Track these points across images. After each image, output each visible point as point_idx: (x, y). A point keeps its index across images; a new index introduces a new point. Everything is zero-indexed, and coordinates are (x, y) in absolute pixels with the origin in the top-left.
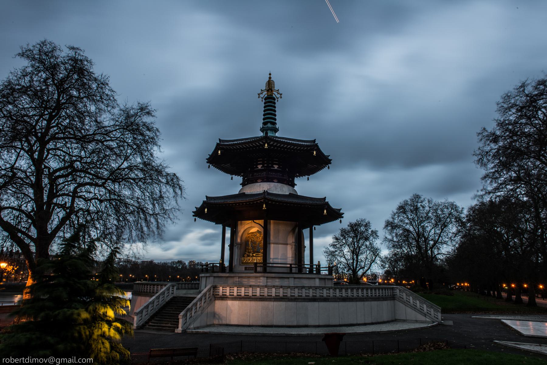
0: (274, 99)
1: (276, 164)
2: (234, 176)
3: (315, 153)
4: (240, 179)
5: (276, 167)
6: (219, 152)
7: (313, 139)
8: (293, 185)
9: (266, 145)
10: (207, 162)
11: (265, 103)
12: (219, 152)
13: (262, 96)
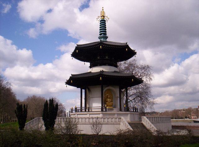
2: (85, 62)
3: (127, 49)
4: (88, 64)
8: (116, 66)
10: (71, 56)
13: (98, 19)
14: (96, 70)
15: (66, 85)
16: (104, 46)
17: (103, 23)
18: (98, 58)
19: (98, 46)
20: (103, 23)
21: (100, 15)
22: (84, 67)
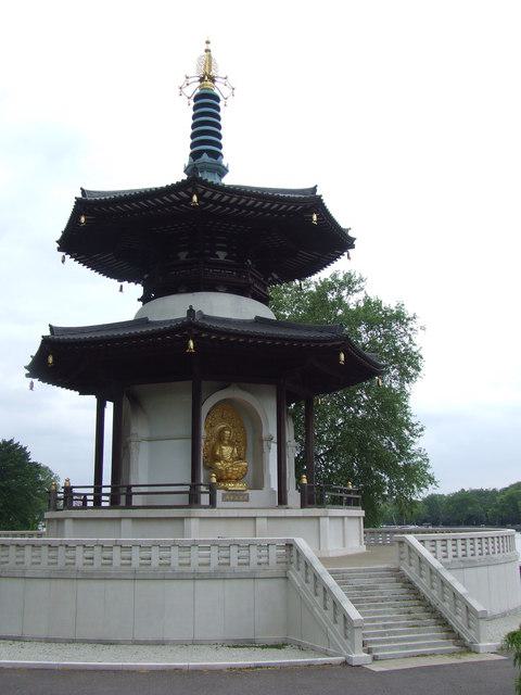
0: (218, 99)
1: (222, 249)
2: (125, 284)
3: (315, 217)
4: (137, 290)
5: (222, 255)
6: (83, 219)
7: (313, 186)
9: (195, 198)
10: (59, 250)
11: (195, 108)
12: (83, 219)
14: (173, 308)
15: (30, 380)
16: (208, 194)
17: (206, 111)
18: (183, 256)
19: (182, 193)
20: (206, 111)
21: (194, 72)
22: (110, 302)
